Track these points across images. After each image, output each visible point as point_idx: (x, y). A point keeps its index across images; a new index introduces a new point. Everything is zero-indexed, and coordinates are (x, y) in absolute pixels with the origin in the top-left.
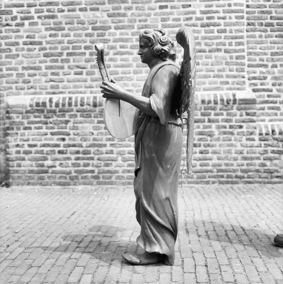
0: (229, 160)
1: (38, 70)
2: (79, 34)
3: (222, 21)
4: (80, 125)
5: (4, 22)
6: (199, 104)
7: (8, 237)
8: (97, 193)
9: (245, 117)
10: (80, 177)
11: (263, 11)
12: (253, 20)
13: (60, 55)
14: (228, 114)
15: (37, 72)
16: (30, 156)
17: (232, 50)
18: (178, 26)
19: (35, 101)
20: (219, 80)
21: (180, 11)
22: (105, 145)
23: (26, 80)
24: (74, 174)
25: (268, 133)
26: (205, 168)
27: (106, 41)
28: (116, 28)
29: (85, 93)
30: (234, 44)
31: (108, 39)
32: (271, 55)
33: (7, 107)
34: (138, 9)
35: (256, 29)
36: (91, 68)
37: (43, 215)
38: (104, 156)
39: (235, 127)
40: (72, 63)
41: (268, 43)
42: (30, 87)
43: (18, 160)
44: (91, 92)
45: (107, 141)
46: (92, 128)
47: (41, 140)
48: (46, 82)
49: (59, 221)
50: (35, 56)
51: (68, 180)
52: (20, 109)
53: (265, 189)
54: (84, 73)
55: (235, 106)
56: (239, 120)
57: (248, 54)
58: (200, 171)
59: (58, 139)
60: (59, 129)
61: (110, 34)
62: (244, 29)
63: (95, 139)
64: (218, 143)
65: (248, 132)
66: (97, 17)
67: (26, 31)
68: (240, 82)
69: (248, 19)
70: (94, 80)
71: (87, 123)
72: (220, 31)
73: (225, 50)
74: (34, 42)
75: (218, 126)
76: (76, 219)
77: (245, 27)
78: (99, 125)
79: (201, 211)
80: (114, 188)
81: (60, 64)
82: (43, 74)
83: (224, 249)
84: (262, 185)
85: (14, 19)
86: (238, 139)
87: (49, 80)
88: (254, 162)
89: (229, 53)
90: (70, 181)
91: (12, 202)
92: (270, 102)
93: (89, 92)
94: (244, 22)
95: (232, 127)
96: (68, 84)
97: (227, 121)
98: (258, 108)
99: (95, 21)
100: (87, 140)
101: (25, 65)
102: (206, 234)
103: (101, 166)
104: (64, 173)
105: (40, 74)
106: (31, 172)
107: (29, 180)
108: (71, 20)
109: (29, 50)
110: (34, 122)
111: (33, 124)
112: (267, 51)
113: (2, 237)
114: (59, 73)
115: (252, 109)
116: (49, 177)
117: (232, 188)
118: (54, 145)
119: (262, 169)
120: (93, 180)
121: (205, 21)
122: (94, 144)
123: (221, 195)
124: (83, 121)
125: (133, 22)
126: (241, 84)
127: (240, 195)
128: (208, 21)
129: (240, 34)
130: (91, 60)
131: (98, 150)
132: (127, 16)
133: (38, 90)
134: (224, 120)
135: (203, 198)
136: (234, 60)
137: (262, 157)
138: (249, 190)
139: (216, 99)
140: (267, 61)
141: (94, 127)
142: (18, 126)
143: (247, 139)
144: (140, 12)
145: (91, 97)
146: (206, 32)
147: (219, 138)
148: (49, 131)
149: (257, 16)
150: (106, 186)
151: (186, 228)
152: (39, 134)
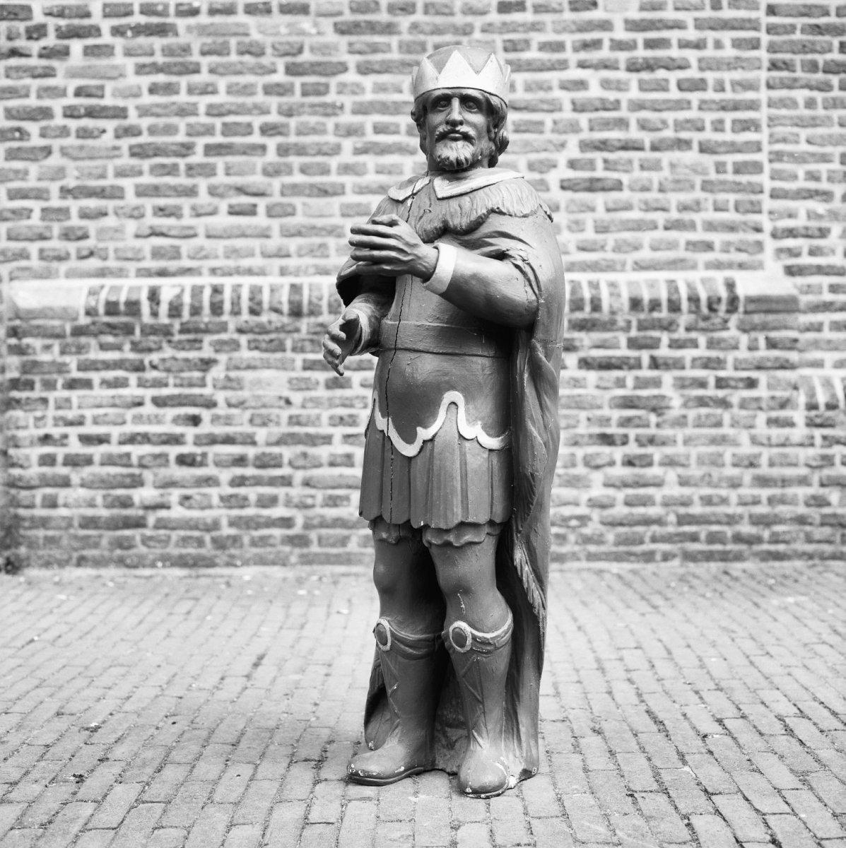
0: (716, 486)
1: (112, 197)
2: (245, 87)
3: (692, 55)
4: (248, 375)
5: (6, 45)
6: (621, 310)
7: (69, 745)
8: (309, 592)
9: (763, 353)
10: (246, 540)
11: (818, 26)
12: (787, 52)
13: (184, 151)
14: (711, 344)
15: (110, 205)
16: (87, 472)
17: (724, 143)
18: (557, 66)
19: (103, 296)
20: (682, 237)
21: (565, 21)
22: (327, 440)
23: (72, 229)
24: (227, 531)
25: (835, 402)
26: (640, 510)
27: (329, 111)
28: (364, 70)
29: (262, 272)
30: (728, 125)
31: (338, 104)
32: (842, 163)
33: (12, 315)
34: (432, 11)
35: (795, 80)
36: (283, 194)
37: (159, 666)
38: (326, 472)
39: (732, 383)
40: (221, 179)
41: (832, 125)
42: (85, 253)
43: (48, 485)
44: (283, 272)
45: (334, 425)
46: (288, 385)
47: (124, 423)
48: (137, 236)
49: (221, 686)
50: (104, 153)
51: (208, 550)
52: (56, 323)
53: (831, 576)
54: (261, 209)
55: (734, 320)
56: (745, 361)
57: (772, 157)
58: (625, 521)
59: (176, 420)
60: (181, 385)
61: (342, 89)
62: (759, 80)
63: (294, 420)
64: (680, 434)
65: (773, 398)
66: (302, 33)
67: (73, 74)
68: (748, 243)
69: (772, 48)
70: (293, 231)
71: (269, 368)
72: (685, 85)
73: (700, 144)
74: (98, 109)
75: (682, 379)
76: (275, 679)
77: (763, 75)
78: (308, 374)
79: (669, 653)
80: (357, 575)
81: (182, 180)
82: (124, 210)
83: (804, 782)
84: (814, 566)
85: (35, 36)
86: (743, 422)
87: (148, 232)
88: (790, 491)
89: (714, 152)
90: (214, 552)
91: (44, 623)
92: (838, 306)
93: (276, 270)
94: (759, 59)
95: (723, 383)
96: (209, 244)
97: (707, 364)
98: (802, 327)
99: (297, 46)
100: (271, 421)
101: (71, 183)
102: (720, 729)
103: (313, 506)
104: (196, 528)
105: (120, 212)
106: (89, 523)
107: (83, 548)
108: (220, 40)
109: (84, 134)
110: (99, 366)
111: (97, 369)
112: (828, 149)
113: (47, 746)
114: (179, 208)
115: (786, 328)
116: (146, 541)
117: (726, 573)
118: (164, 438)
119: (815, 513)
120: (287, 549)
121: (641, 53)
122: (292, 435)
123: (703, 596)
124: (258, 363)
125: (417, 53)
126: (750, 250)
127: (763, 596)
128: (650, 54)
129: (750, 95)
130: (283, 168)
131: (305, 455)
132: (399, 33)
133: (112, 263)
134: (699, 362)
135: (655, 607)
136: (730, 177)
137: (815, 479)
138: (786, 582)
139: (674, 297)
140: (830, 179)
141: (295, 382)
142: (47, 377)
143: (771, 422)
144: (439, 20)
145: (282, 286)
146: (645, 87)
147: (684, 417)
148: (149, 393)
149: (800, 41)
150: (328, 569)
151: (645, 708)
152: (118, 401)
